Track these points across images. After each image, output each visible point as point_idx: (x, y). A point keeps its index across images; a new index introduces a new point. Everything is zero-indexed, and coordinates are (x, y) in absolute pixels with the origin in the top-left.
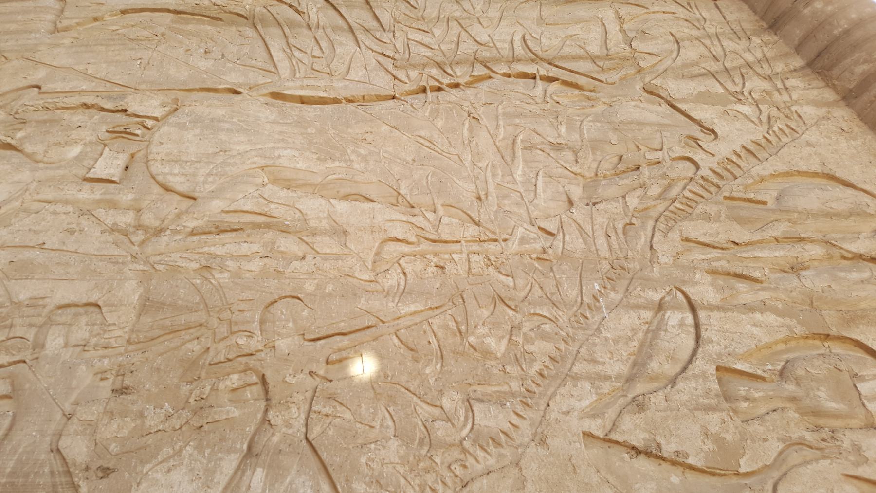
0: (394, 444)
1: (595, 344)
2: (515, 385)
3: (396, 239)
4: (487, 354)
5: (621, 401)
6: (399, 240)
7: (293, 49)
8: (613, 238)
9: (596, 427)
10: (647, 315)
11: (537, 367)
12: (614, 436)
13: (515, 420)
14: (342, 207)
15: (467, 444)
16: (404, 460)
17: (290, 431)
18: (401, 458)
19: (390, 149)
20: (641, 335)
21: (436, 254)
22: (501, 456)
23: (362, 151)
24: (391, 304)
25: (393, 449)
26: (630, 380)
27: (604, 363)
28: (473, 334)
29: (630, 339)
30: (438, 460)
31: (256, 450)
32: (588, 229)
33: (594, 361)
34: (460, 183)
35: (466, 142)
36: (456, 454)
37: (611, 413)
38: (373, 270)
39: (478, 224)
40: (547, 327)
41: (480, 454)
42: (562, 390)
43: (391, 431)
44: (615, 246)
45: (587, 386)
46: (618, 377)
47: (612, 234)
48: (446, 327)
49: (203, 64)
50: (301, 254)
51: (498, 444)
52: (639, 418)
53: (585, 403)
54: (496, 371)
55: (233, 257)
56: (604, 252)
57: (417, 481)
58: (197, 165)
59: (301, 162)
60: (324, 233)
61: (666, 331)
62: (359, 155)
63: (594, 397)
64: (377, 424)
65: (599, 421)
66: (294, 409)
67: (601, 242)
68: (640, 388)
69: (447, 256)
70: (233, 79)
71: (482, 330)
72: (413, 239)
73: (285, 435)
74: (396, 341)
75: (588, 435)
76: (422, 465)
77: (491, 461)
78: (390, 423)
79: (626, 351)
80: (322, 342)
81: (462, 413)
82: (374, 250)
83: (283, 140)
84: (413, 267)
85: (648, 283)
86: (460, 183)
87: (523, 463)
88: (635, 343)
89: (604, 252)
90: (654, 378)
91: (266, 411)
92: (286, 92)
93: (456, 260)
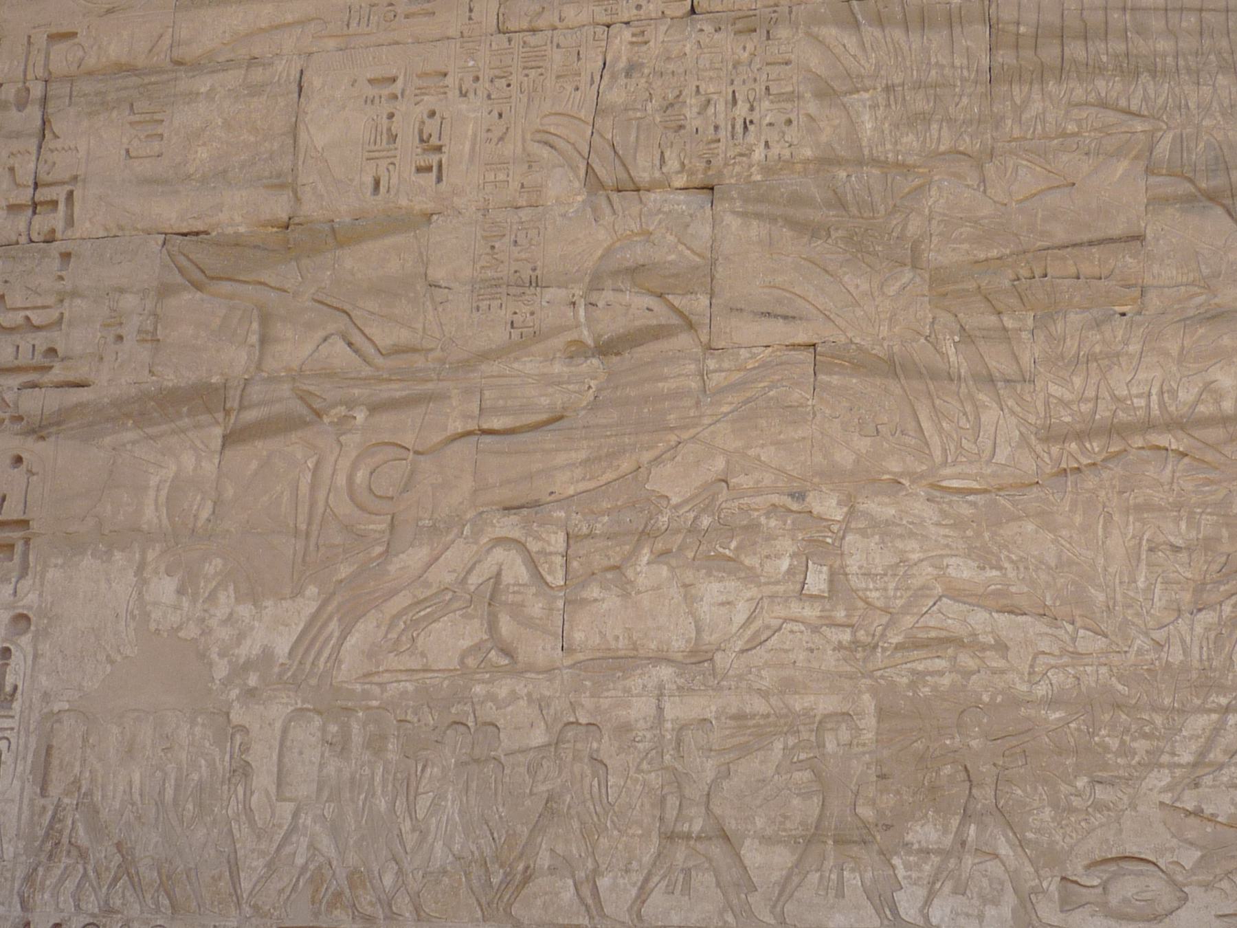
0: (1047, 810)
1: (1176, 741)
2: (1121, 772)
3: (1043, 653)
4: (1107, 749)
5: (1187, 781)
6: (1046, 654)
7: (940, 415)
8: (1205, 649)
9: (1167, 798)
10: (1214, 716)
11: (1137, 759)
12: (1178, 804)
13: (1120, 794)
14: (1002, 619)
15: (1090, 810)
16: (1053, 819)
17: (987, 802)
18: (1052, 818)
19: (1036, 553)
20: (1208, 733)
21: (1073, 666)
22: (1109, 816)
23: (1013, 557)
24: (1043, 712)
25: (1048, 813)
26: (1195, 765)
27: (1179, 756)
28: (1098, 735)
29: (1199, 737)
30: (1073, 819)
31: (969, 812)
32: (1188, 639)
33: (1173, 754)
34: (1093, 591)
35: (1100, 543)
36: (1084, 816)
37: (1179, 788)
38: (1029, 681)
39: (1106, 636)
40: (1147, 729)
41: (1098, 815)
42: (1151, 775)
43: (1046, 803)
44: (1205, 657)
45: (1167, 771)
46: (1188, 763)
47: (1204, 644)
48: (1079, 730)
49: (863, 444)
50: (976, 668)
51: (1109, 809)
52: (1195, 792)
53: (1163, 783)
54: (1110, 762)
55: (932, 674)
56: (1196, 664)
57: (1062, 831)
58: (886, 579)
59: (965, 572)
60: (991, 647)
61: (1225, 730)
62: (1012, 561)
63: (1169, 779)
64: (1036, 798)
65: (1170, 795)
66: (987, 789)
67: (1196, 651)
68: (1200, 772)
69: (1082, 669)
70: (894, 466)
71: (1103, 732)
72: (1057, 652)
73: (984, 805)
74: (1047, 740)
75: (1161, 803)
76: (1063, 822)
77: (1104, 820)
78: (1045, 797)
79: (1194, 747)
80: (999, 741)
81: (1088, 789)
82: (1029, 662)
83: (947, 546)
84: (1055, 677)
85: (1222, 689)
86: (1093, 591)
87: (1122, 821)
88: (1203, 740)
89: (1196, 664)
90: (1211, 764)
91: (970, 789)
92: (945, 484)
93: (1089, 672)
